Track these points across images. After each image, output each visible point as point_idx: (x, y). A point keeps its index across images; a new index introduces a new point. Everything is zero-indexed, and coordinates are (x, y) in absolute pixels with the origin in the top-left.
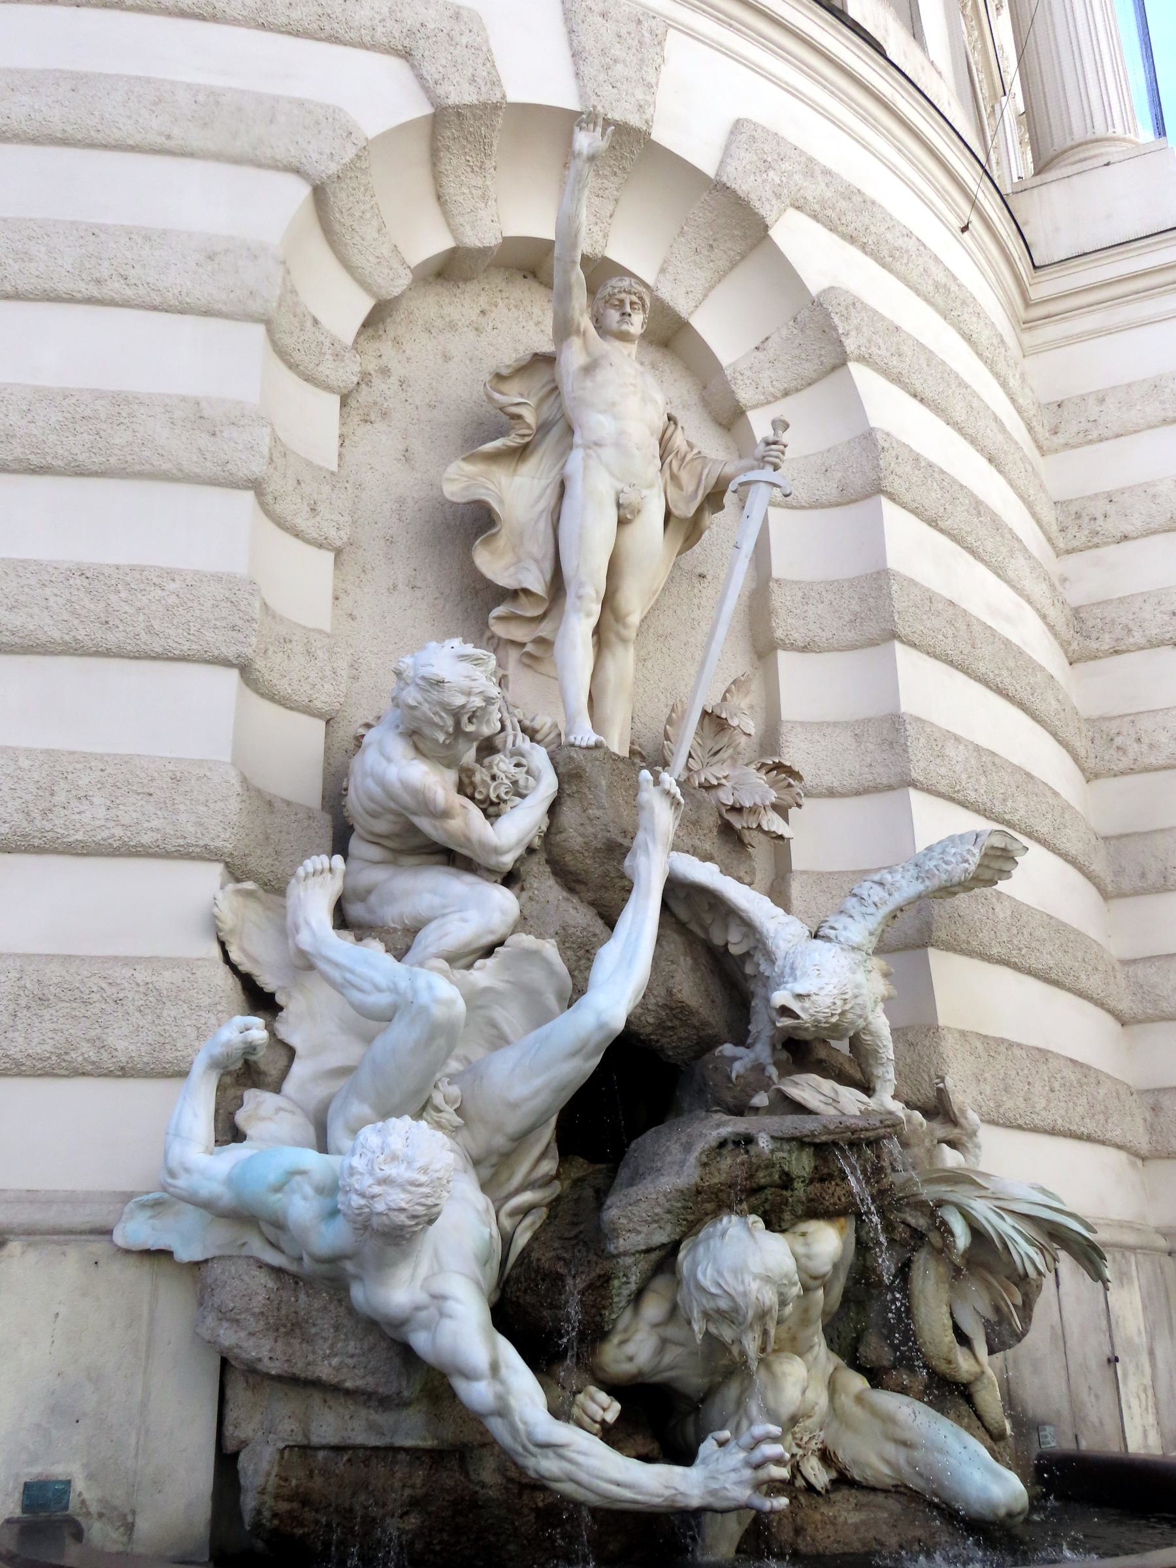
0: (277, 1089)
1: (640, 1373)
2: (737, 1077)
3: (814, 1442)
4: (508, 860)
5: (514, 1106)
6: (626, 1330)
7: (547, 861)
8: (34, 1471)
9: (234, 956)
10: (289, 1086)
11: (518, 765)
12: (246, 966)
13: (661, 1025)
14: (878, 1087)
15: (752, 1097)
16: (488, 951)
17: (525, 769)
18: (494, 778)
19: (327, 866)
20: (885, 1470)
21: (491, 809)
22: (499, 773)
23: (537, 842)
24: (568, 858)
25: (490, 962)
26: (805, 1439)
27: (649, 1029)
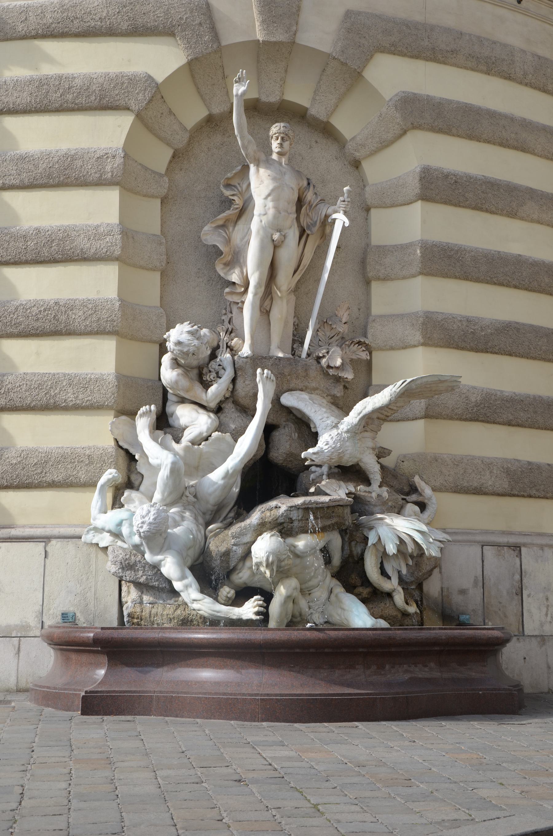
0: (138, 489)
1: (245, 583)
2: (313, 480)
4: (213, 405)
5: (210, 495)
6: (240, 569)
7: (233, 402)
8: (65, 609)
9: (121, 443)
10: (142, 488)
11: (220, 365)
12: (125, 446)
13: (285, 460)
14: (372, 482)
15: (309, 489)
16: (207, 439)
17: (221, 367)
18: (210, 371)
19: (148, 409)
20: (338, 618)
21: (206, 385)
22: (211, 370)
23: (227, 396)
24: (240, 400)
25: (207, 442)
26: (316, 608)
27: (281, 462)
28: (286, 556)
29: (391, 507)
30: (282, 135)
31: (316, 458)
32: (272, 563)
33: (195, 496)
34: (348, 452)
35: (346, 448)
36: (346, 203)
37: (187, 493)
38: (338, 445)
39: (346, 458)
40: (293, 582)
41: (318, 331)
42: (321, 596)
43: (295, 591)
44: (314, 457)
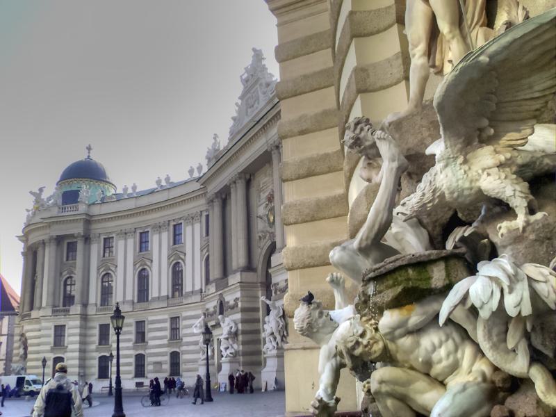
28: (353, 344)
29: (536, 240)
34: (444, 187)
43: (384, 385)
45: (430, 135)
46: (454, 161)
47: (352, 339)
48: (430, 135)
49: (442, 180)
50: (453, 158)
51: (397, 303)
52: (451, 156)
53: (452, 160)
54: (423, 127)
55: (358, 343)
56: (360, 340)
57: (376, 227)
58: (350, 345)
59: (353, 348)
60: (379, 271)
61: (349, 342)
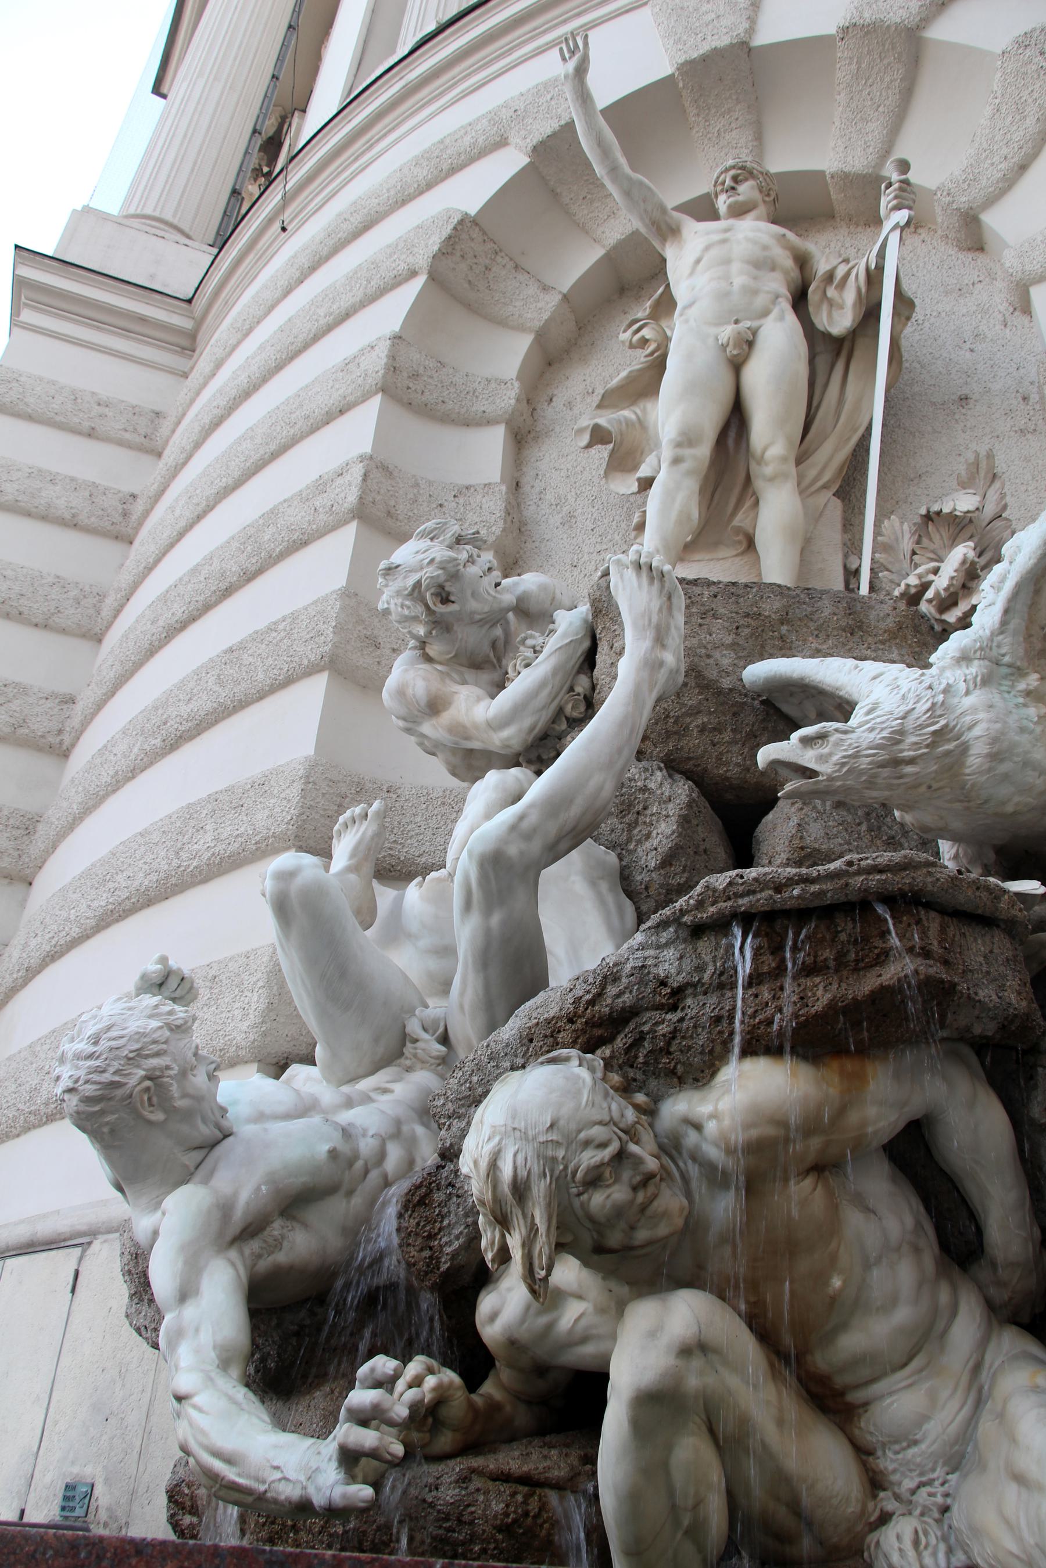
3: (928, 1489)
26: (908, 1484)
28: (607, 1153)
30: (733, 172)
31: (822, 759)
32: (520, 1190)
33: (445, 1039)
34: (977, 731)
35: (968, 719)
36: (896, 186)
37: (414, 1027)
38: (923, 706)
39: (975, 760)
40: (684, 1313)
41: (914, 553)
42: (925, 1418)
44: (808, 758)
45: (733, 646)
46: (1005, 677)
47: (597, 1132)
48: (733, 646)
49: (974, 710)
50: (1009, 666)
51: (812, 1041)
52: (1007, 659)
53: (1004, 670)
54: (715, 617)
55: (621, 1156)
56: (633, 1148)
57: (575, 811)
58: (589, 1158)
59: (594, 1180)
60: (814, 888)
61: (587, 1144)
